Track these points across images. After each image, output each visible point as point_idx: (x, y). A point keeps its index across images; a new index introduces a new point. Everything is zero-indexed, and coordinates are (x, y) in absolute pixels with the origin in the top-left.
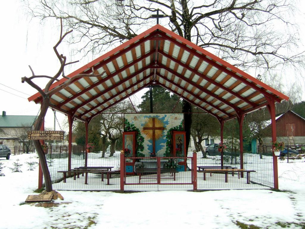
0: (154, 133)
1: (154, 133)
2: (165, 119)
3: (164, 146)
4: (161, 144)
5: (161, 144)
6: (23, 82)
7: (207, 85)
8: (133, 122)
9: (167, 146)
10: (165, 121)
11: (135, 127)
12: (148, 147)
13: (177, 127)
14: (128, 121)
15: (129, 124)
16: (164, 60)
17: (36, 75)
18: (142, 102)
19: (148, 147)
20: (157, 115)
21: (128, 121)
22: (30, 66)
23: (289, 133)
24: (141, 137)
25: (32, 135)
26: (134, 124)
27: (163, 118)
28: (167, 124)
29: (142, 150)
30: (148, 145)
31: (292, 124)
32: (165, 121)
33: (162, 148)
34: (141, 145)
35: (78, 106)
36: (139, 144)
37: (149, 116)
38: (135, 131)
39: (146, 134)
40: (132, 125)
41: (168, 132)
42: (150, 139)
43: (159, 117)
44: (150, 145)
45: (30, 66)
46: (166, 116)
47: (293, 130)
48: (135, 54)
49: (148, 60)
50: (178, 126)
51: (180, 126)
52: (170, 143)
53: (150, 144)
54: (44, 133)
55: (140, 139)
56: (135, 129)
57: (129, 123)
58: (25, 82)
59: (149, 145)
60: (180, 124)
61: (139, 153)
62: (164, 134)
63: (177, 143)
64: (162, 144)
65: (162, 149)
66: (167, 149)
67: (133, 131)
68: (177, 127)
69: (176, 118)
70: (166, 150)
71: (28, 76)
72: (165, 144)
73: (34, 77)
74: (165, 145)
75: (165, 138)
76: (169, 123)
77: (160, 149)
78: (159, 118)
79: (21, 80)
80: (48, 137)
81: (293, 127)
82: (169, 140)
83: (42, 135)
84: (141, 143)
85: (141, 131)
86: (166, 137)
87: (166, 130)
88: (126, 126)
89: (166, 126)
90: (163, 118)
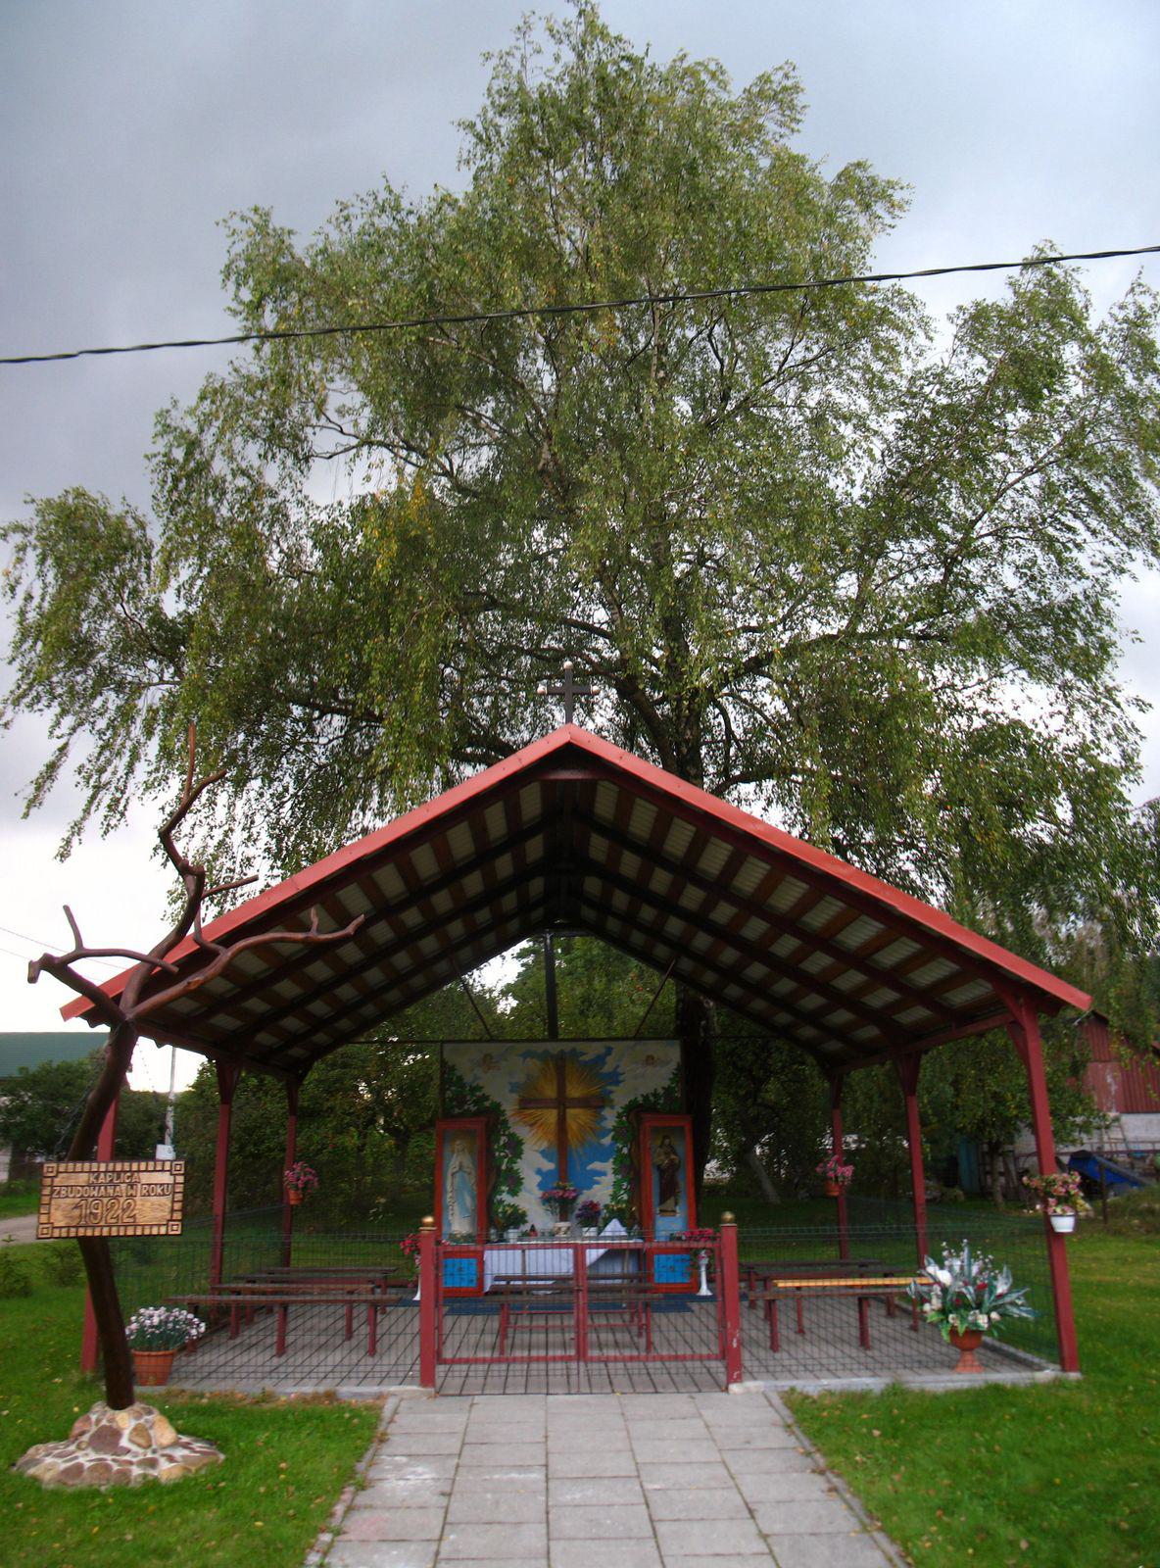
0: (562, 1120)
1: (562, 1120)
2: (604, 1063)
3: (604, 1174)
4: (589, 1167)
5: (589, 1167)
6: (32, 979)
7: (770, 938)
8: (476, 1078)
9: (615, 1172)
10: (607, 1069)
11: (486, 1098)
12: (538, 1179)
13: (655, 1094)
14: (458, 1073)
15: (463, 1086)
16: (598, 847)
17: (88, 945)
18: (519, 975)
19: (538, 1179)
20: (574, 1050)
21: (458, 1073)
22: (67, 909)
23: (1100, 1098)
24: (511, 1136)
25: (57, 1181)
26: (481, 1083)
27: (600, 1060)
28: (617, 1083)
29: (514, 1192)
30: (539, 1172)
31: (1109, 1066)
32: (607, 1069)
33: (598, 1183)
34: (510, 1170)
35: (261, 1023)
36: (504, 1167)
37: (540, 1051)
38: (487, 1110)
39: (532, 1125)
40: (473, 1090)
41: (619, 1116)
42: (545, 1144)
43: (583, 1054)
44: (551, 1171)
45: (67, 909)
46: (609, 1051)
47: (1114, 1088)
48: (485, 830)
49: (535, 848)
50: (661, 1091)
51: (668, 1091)
52: (627, 1162)
53: (549, 1166)
54: (106, 1172)
55: (505, 1146)
56: (487, 1104)
57: (460, 1078)
58: (44, 975)
59: (545, 1169)
60: (666, 1083)
61: (501, 1202)
62: (603, 1124)
63: (657, 1160)
64: (597, 1165)
65: (596, 1186)
66: (617, 1185)
67: (477, 1114)
68: (655, 1094)
69: (650, 1060)
70: (611, 1191)
71: (63, 947)
72: (608, 1166)
73: (81, 953)
74: (610, 1172)
75: (607, 1141)
76: (621, 1078)
77: (589, 1188)
78: (582, 1058)
79: (25, 972)
80: (123, 1186)
81: (1114, 1078)
82: (625, 1151)
83: (97, 1178)
84: (512, 1161)
85: (508, 1113)
86: (613, 1138)
87: (612, 1107)
88: (449, 1094)
89: (611, 1092)
90: (600, 1060)
